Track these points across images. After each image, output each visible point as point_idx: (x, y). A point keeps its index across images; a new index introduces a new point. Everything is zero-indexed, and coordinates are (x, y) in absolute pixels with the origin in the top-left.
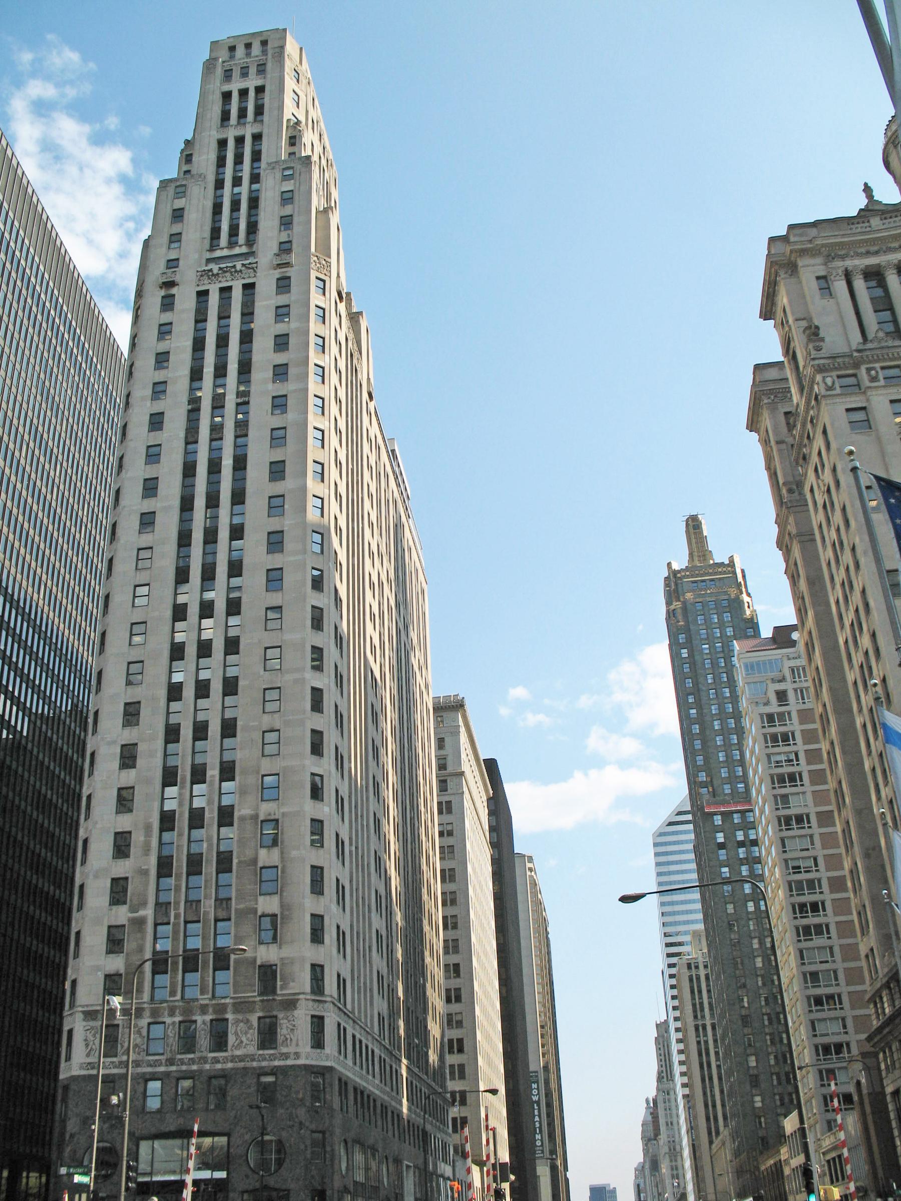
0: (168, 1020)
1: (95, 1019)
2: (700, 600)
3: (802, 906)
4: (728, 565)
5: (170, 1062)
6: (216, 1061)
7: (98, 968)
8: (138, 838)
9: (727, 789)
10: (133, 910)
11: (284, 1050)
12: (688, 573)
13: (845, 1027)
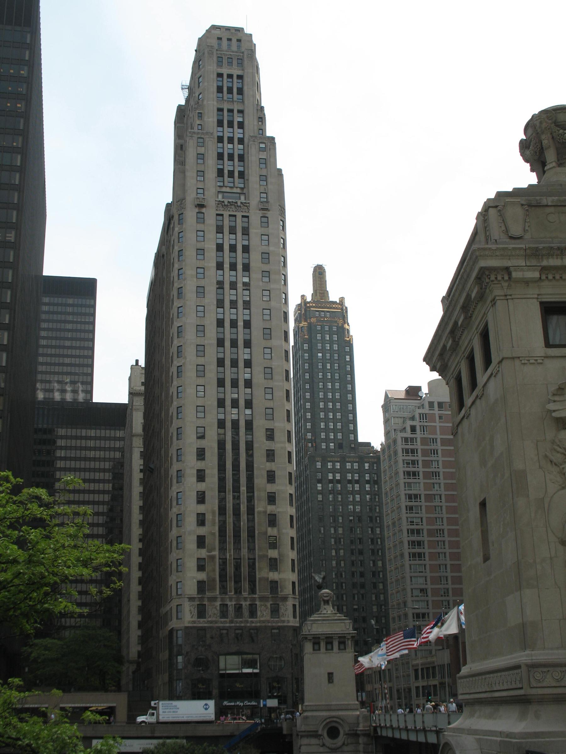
0: (229, 603)
1: (194, 601)
2: (321, 324)
3: (413, 542)
4: (339, 304)
5: (231, 622)
6: (252, 622)
7: (194, 578)
8: (209, 517)
9: (324, 446)
10: (209, 551)
11: (283, 619)
12: (314, 305)
13: (428, 605)
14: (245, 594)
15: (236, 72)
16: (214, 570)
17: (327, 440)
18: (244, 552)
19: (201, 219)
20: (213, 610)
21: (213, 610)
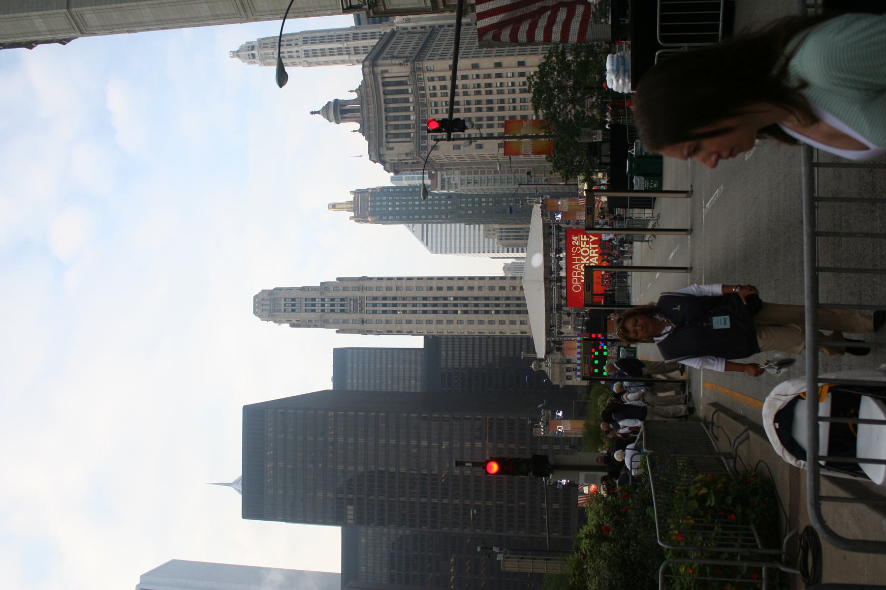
9: (450, 208)
15: (283, 302)
17: (446, 205)
19: (370, 322)
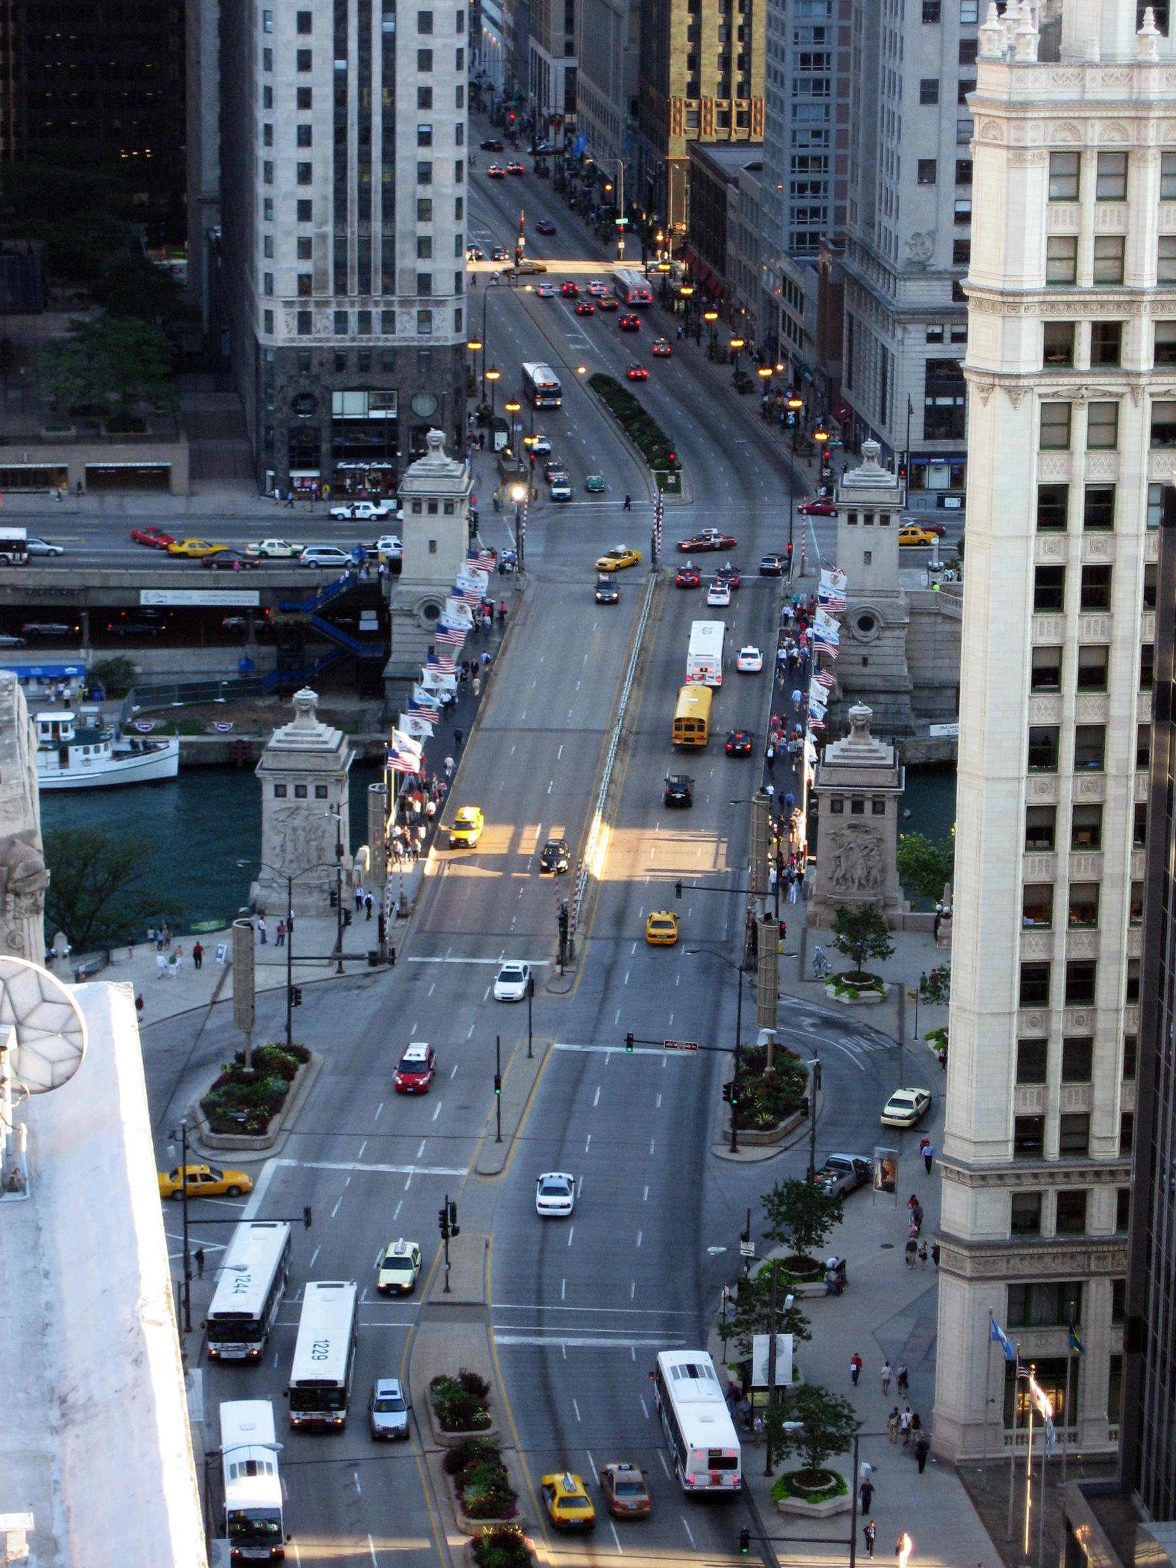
3: (802, 212)
5: (353, 340)
7: (292, 269)
14: (377, 293)
16: (325, 257)
18: (377, 226)
20: (323, 322)
21: (323, 322)
